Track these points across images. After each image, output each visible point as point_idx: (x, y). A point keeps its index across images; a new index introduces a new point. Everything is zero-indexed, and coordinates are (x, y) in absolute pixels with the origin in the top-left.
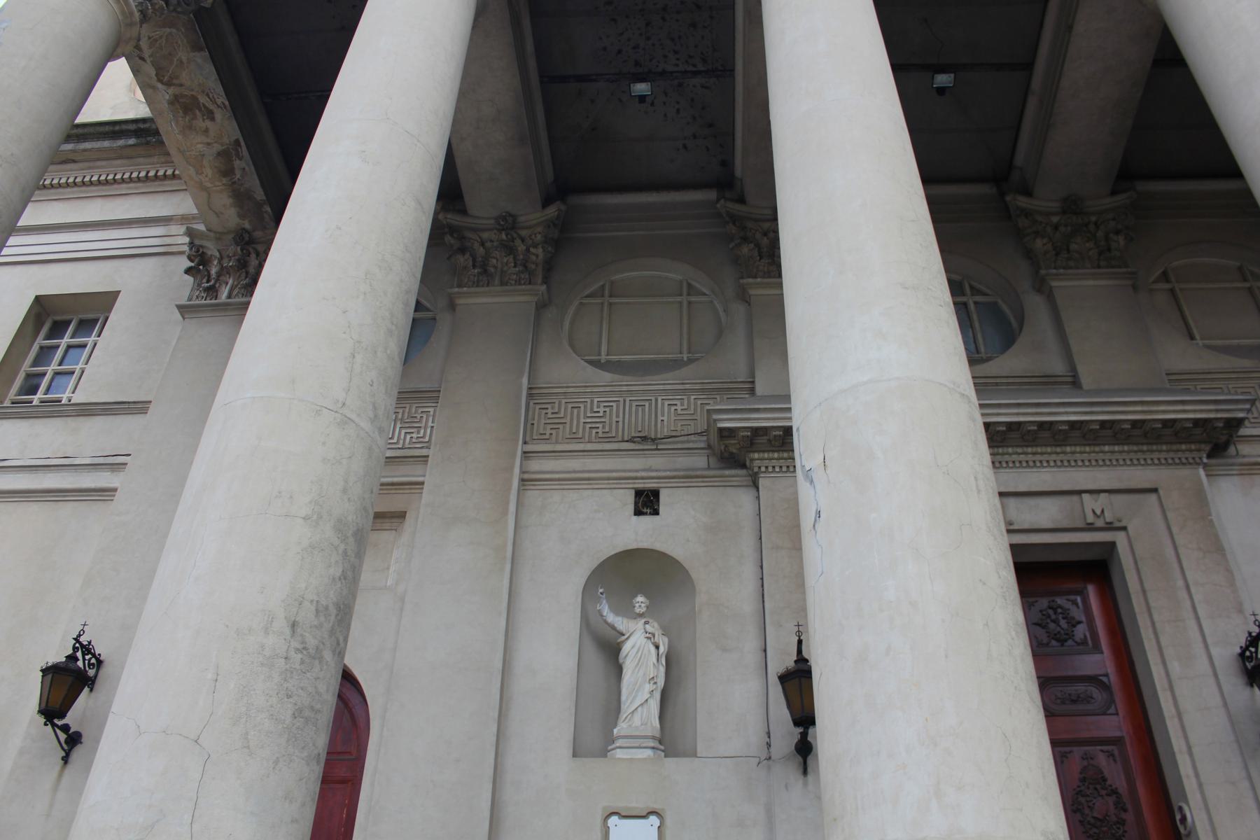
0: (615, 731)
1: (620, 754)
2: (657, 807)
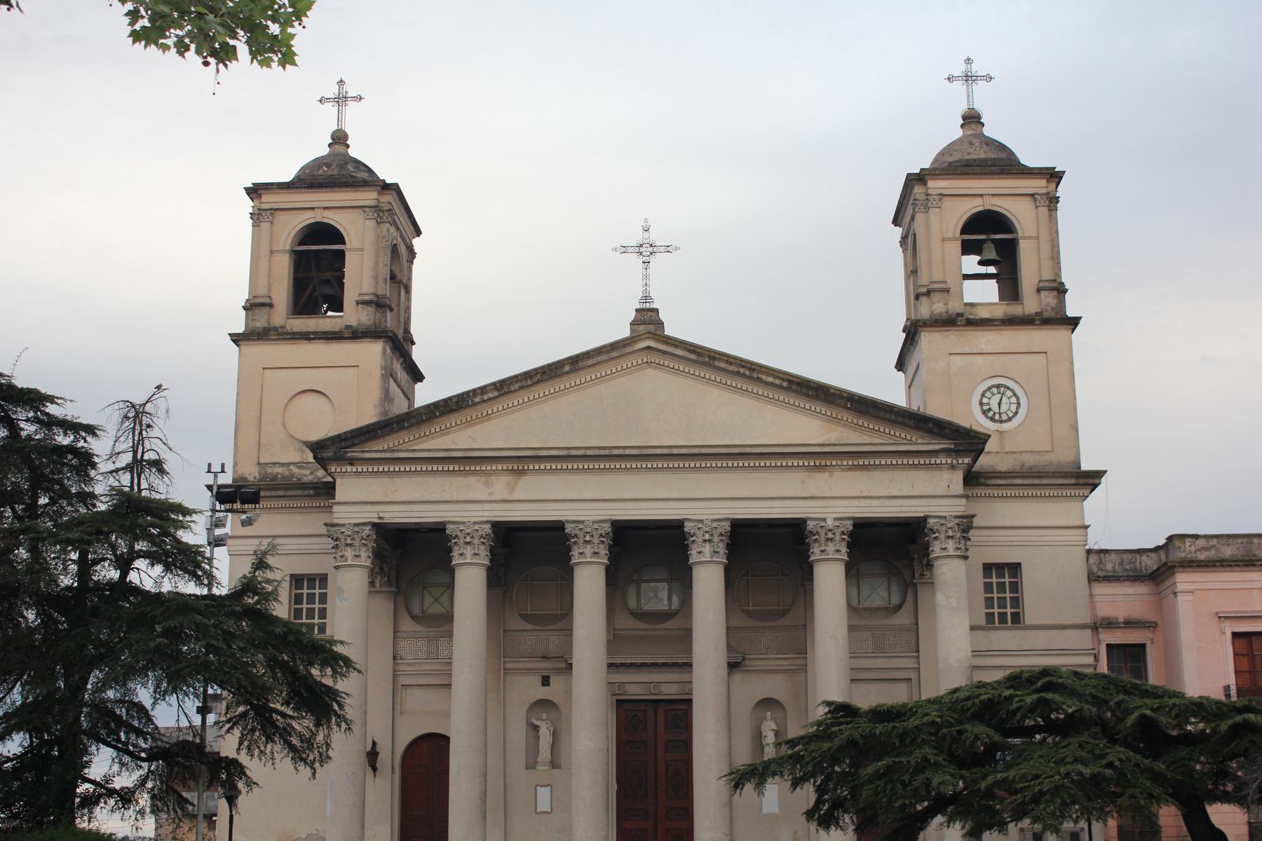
0: (538, 760)
1: (539, 768)
2: (549, 783)
